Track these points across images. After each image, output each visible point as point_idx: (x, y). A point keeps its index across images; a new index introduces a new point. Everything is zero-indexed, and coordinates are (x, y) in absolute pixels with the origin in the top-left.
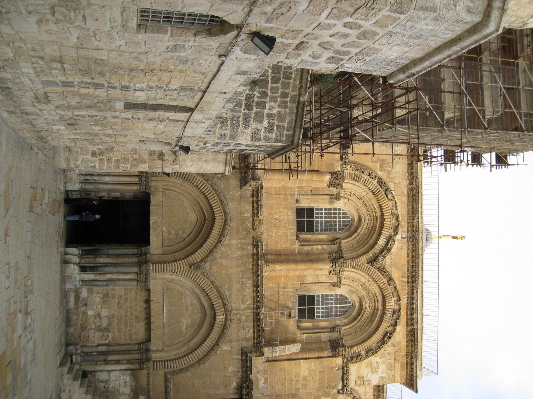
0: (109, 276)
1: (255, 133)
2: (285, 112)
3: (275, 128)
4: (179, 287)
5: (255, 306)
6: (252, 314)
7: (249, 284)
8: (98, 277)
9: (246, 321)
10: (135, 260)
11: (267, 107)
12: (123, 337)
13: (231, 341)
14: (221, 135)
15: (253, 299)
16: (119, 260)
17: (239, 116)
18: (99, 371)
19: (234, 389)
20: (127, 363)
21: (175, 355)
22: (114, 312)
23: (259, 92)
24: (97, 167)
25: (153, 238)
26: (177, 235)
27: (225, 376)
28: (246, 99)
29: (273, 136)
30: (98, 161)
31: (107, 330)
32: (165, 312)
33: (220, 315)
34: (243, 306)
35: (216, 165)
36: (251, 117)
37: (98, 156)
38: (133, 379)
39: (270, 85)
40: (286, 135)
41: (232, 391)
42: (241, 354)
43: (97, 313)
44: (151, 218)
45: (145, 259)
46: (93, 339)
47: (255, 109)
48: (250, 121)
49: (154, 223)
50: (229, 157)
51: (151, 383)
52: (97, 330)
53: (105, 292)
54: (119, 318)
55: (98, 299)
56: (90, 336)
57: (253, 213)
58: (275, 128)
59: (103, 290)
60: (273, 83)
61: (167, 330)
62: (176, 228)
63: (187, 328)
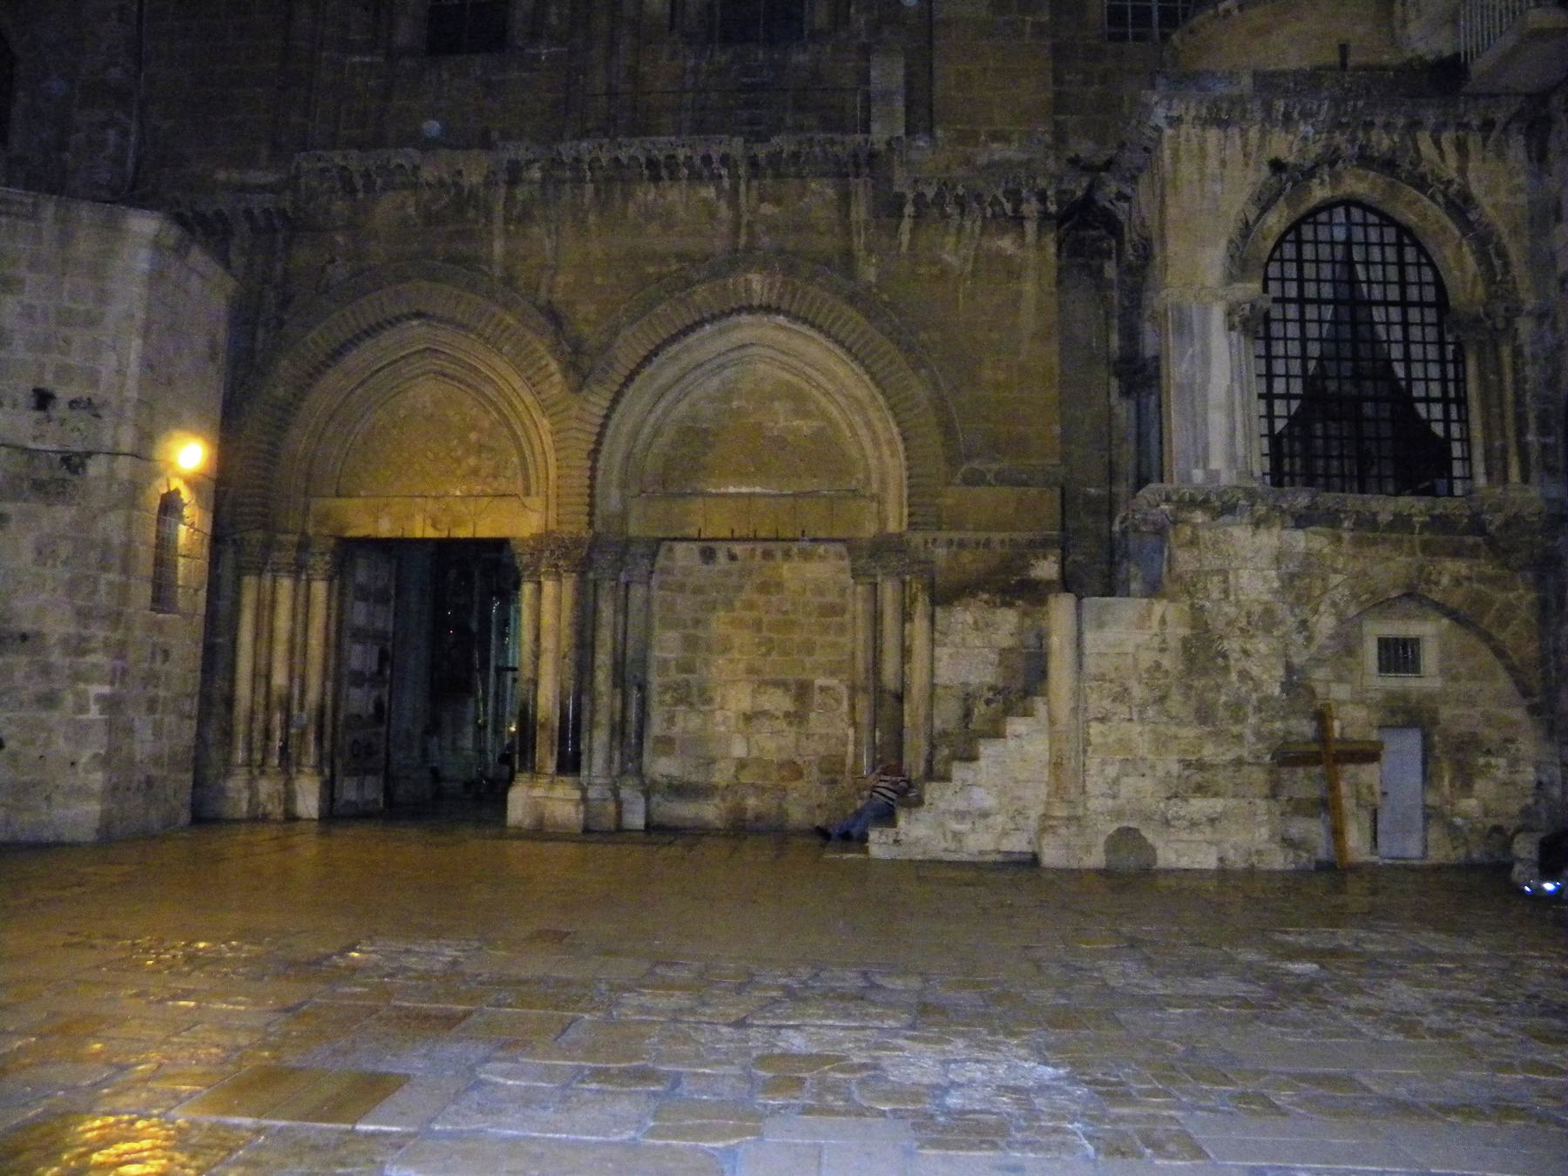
0: (602, 679)
4: (661, 440)
5: (724, 172)
6: (755, 183)
7: (646, 194)
8: (603, 718)
9: (778, 201)
10: (549, 587)
12: (831, 638)
13: (848, 255)
15: (700, 177)
16: (548, 642)
18: (929, 717)
19: (1022, 246)
20: (911, 620)
21: (893, 454)
22: (742, 666)
24: (106, 689)
25: (485, 530)
26: (480, 448)
27: (974, 273)
30: (82, 686)
31: (802, 691)
32: (744, 490)
33: (748, 289)
34: (724, 211)
37: (57, 686)
38: (964, 601)
41: (1031, 255)
42: (894, 221)
43: (741, 724)
44: (418, 534)
45: (547, 553)
46: (834, 741)
49: (434, 526)
51: (982, 536)
52: (801, 723)
53: (668, 698)
54: (763, 649)
55: (695, 722)
56: (822, 750)
57: (404, 186)
59: (662, 703)
61: (809, 484)
62: (460, 453)
63: (807, 415)
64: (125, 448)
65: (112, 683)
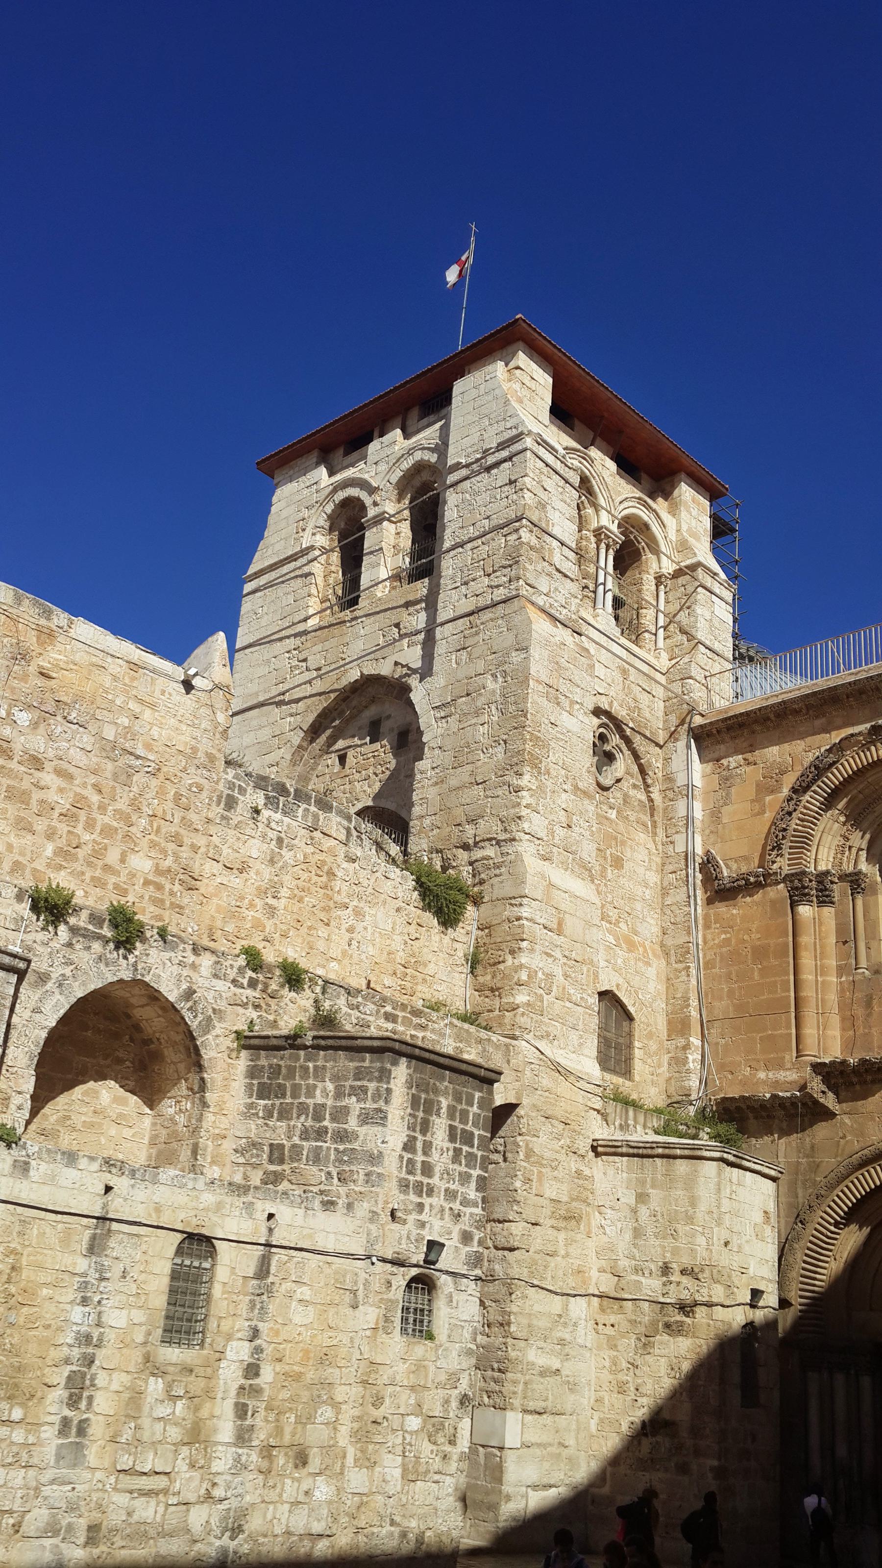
1: (365, 1119)
2: (333, 1067)
3: (359, 1083)
11: (323, 1101)
14: (367, 1182)
17: (336, 1149)
23: (298, 1118)
24: (715, 1463)
28: (306, 1139)
29: (372, 1086)
35: (703, 1179)
36: (339, 1128)
39: (289, 1100)
40: (371, 1062)
47: (326, 1123)
48: (345, 1130)
50: (678, 1152)
58: (359, 1083)
60: (284, 1096)
64: (715, 1300)
65: (719, 1459)
